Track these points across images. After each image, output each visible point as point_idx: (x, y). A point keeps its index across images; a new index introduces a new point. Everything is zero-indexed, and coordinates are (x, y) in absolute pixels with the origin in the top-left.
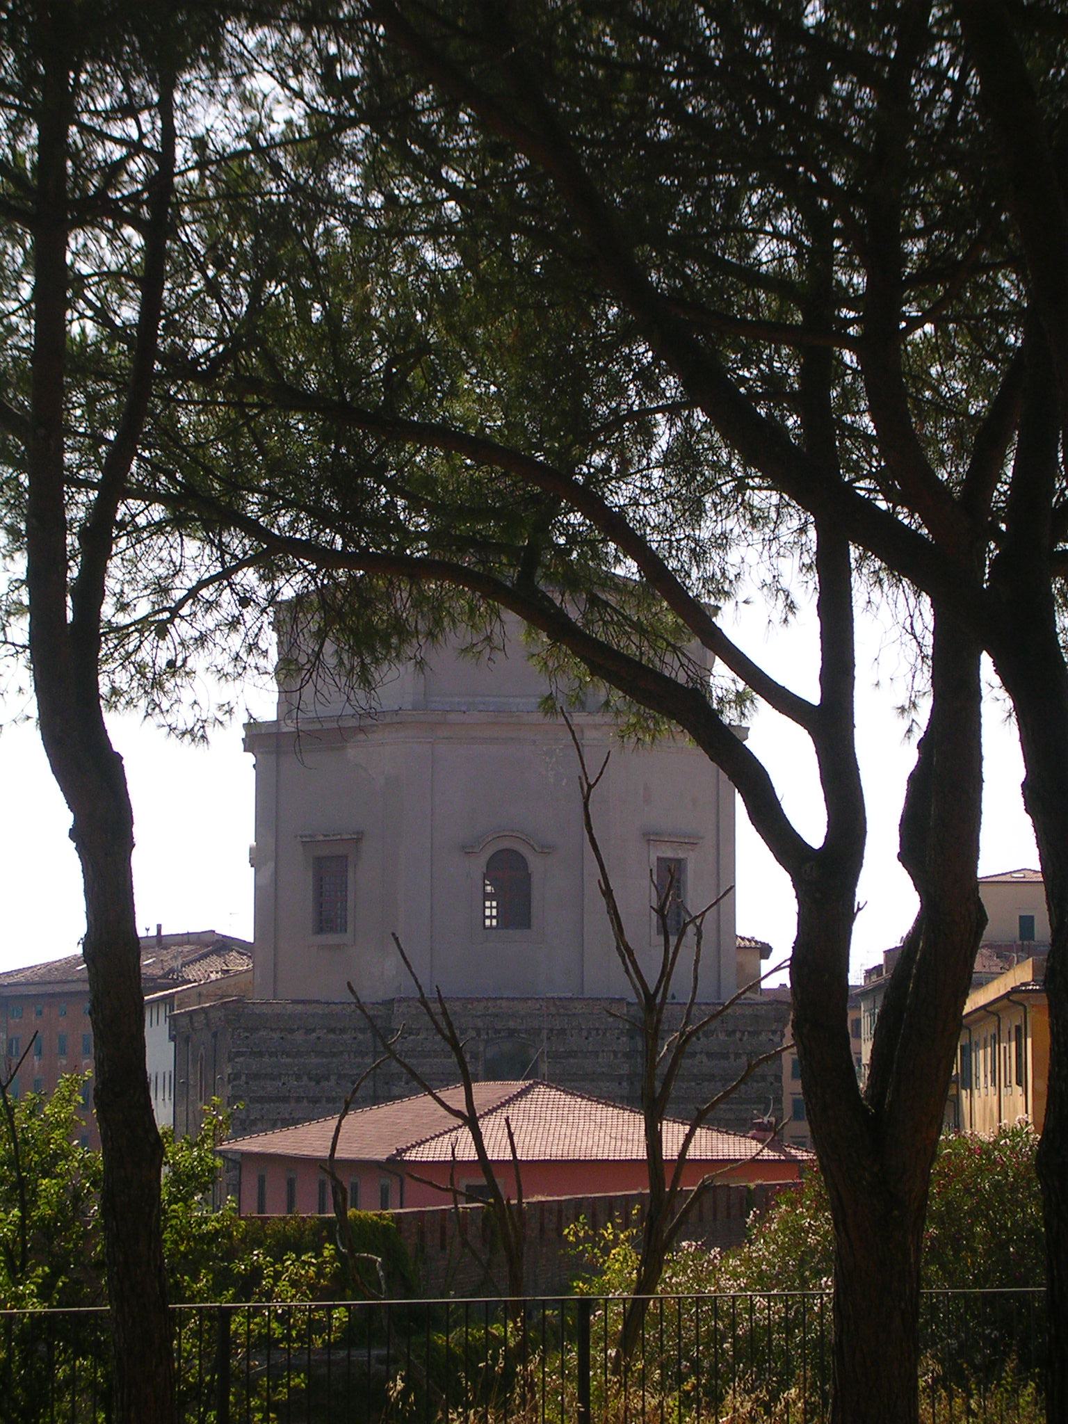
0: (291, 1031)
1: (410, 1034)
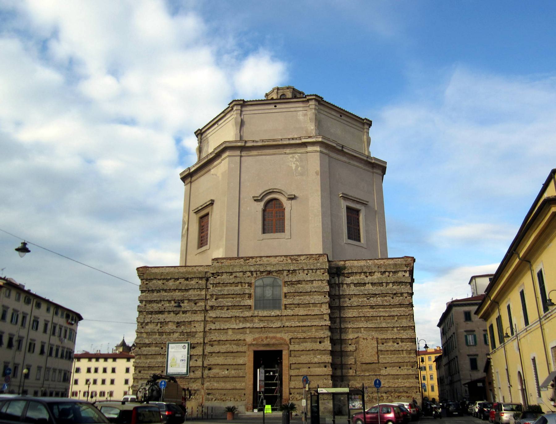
0: (168, 280)
1: (218, 276)
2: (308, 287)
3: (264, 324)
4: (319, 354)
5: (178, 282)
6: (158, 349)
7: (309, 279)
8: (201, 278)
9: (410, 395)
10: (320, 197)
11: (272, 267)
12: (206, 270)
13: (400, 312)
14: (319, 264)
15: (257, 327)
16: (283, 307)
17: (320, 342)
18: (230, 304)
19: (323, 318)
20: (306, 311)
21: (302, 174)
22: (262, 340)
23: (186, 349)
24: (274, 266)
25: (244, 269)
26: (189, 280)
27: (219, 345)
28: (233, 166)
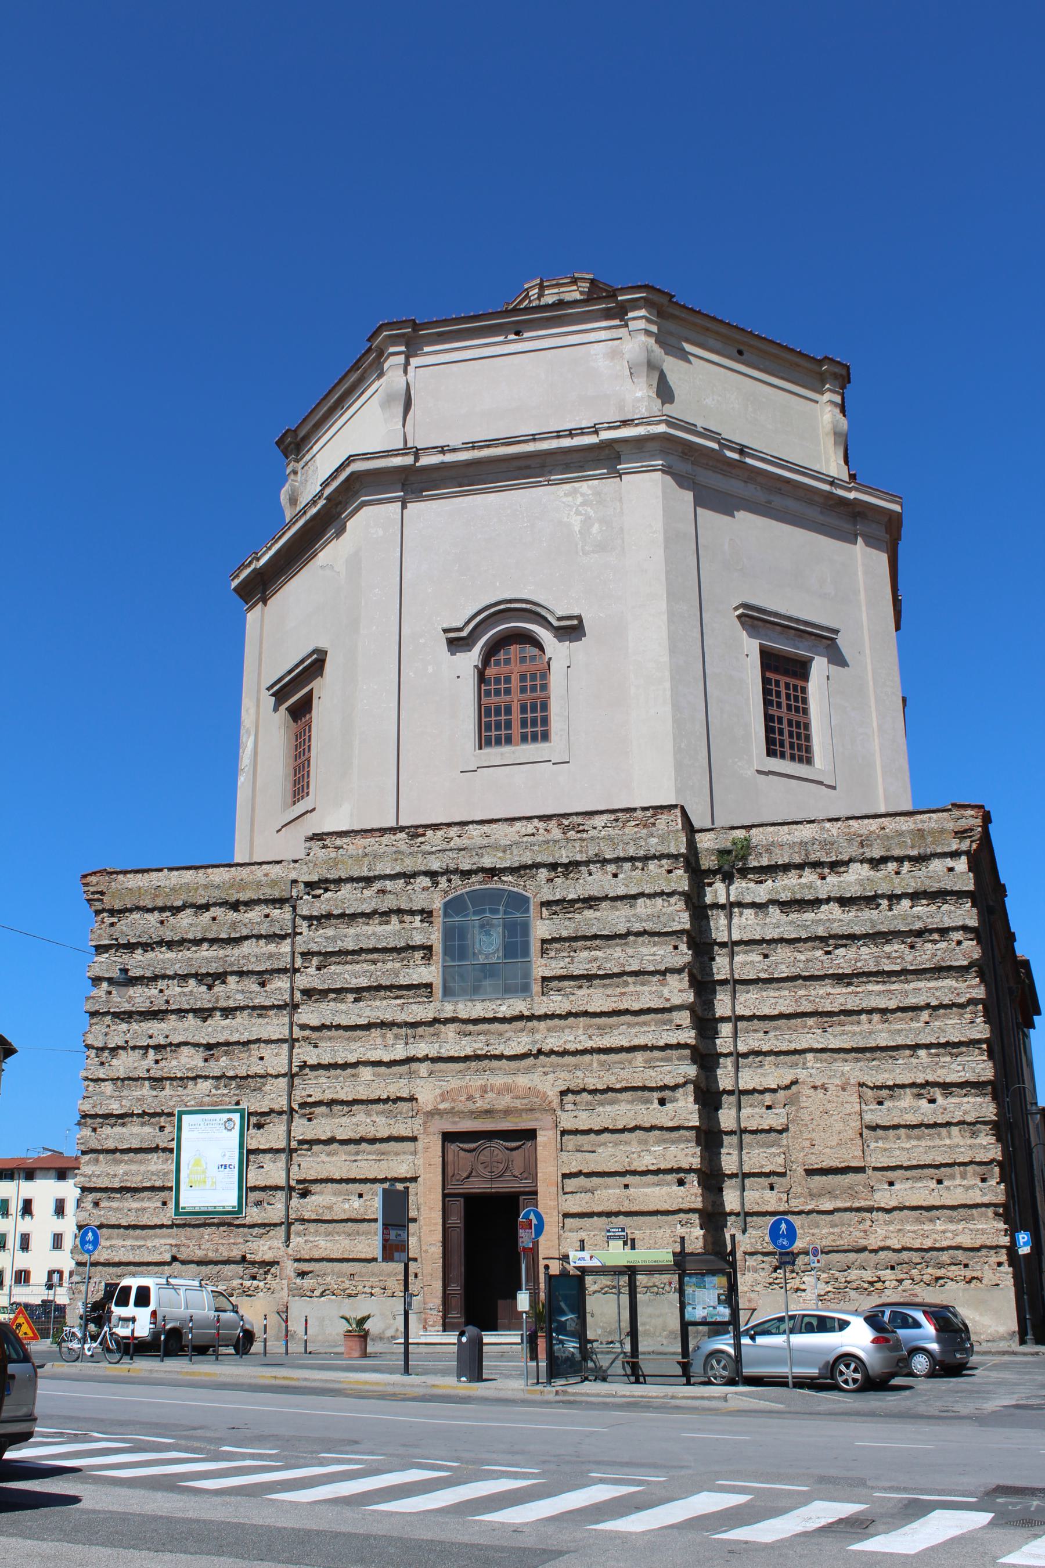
0: (176, 910)
1: (326, 890)
2: (616, 919)
3: (476, 1045)
4: (658, 1142)
5: (208, 915)
6: (151, 1130)
7: (621, 891)
8: (279, 902)
9: (975, 1274)
10: (665, 617)
11: (501, 855)
12: (293, 875)
13: (938, 994)
14: (656, 840)
15: (452, 1053)
16: (536, 988)
17: (662, 1102)
18: (364, 982)
19: (670, 1021)
20: (614, 999)
21: (602, 547)
22: (470, 1098)
23: (236, 1132)
24: (504, 852)
25: (409, 865)
26: (242, 908)
27: (333, 1116)
28: (381, 532)
